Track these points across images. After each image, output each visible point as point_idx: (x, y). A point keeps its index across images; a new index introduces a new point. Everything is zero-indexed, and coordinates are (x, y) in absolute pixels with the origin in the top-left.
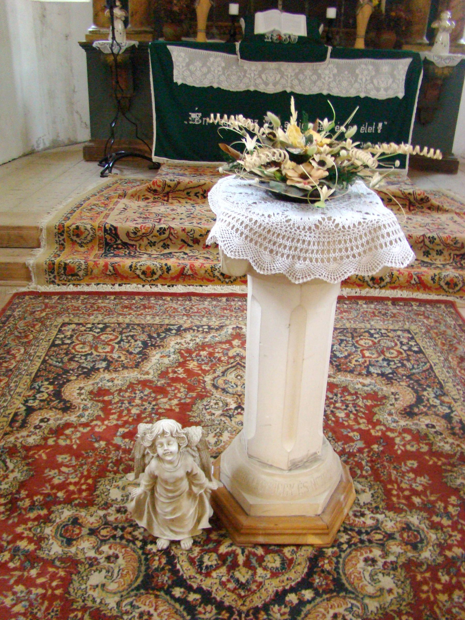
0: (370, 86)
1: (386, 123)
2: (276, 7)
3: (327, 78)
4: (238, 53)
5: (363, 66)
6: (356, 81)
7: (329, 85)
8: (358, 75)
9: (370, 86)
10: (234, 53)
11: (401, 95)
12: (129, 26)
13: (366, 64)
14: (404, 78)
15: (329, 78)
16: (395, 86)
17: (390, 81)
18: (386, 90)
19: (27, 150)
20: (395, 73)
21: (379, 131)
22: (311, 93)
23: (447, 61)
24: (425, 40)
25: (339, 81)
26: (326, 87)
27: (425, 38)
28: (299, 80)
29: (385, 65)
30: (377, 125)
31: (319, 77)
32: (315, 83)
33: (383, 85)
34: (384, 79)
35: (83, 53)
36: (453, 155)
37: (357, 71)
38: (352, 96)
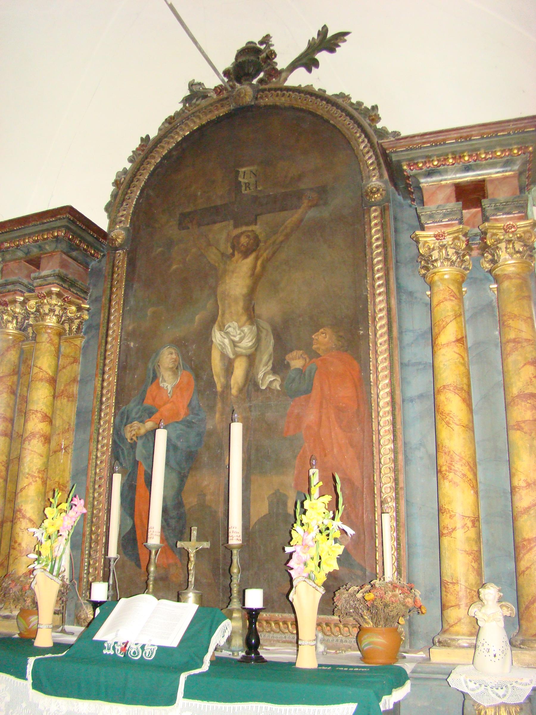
2: (144, 589)
4: (29, 676)
10: (22, 675)
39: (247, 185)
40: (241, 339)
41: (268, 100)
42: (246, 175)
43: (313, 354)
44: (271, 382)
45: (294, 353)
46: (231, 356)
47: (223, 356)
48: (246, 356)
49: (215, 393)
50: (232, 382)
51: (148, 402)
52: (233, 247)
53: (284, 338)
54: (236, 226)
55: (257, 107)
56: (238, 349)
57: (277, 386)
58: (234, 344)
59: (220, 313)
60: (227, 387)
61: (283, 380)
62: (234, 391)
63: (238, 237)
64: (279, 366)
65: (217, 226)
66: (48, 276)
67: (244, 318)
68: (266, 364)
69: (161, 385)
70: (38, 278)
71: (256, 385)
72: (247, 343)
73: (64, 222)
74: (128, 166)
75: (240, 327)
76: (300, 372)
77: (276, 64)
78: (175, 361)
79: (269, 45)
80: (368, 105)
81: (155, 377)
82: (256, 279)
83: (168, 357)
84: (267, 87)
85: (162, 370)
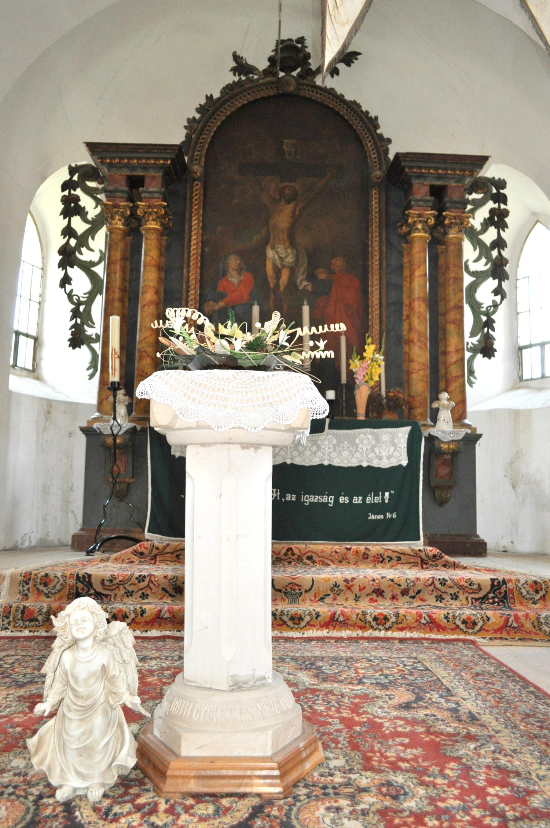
0: (371, 455)
1: (392, 492)
3: (327, 449)
5: (363, 436)
6: (356, 451)
7: (329, 455)
8: (357, 446)
9: (371, 455)
11: (405, 463)
12: (133, 413)
13: (365, 434)
14: (406, 445)
15: (329, 448)
16: (397, 454)
17: (392, 449)
18: (389, 458)
19: (11, 545)
20: (396, 441)
21: (387, 501)
22: (312, 464)
23: (452, 435)
24: (429, 422)
25: (340, 451)
26: (327, 458)
27: (429, 420)
28: (299, 451)
29: (385, 434)
30: (383, 495)
31: (319, 447)
32: (315, 453)
33: (384, 454)
34: (385, 448)
35: (82, 439)
36: (478, 536)
37: (357, 441)
38: (354, 465)
39: (290, 154)
40: (286, 257)
41: (306, 93)
42: (288, 145)
43: (331, 272)
44: (305, 286)
45: (320, 270)
46: (280, 267)
47: (275, 266)
48: (289, 267)
49: (270, 288)
50: (281, 282)
51: (220, 289)
52: (280, 195)
53: (315, 259)
54: (282, 181)
55: (298, 97)
56: (284, 263)
57: (309, 288)
58: (281, 259)
59: (272, 237)
60: (277, 285)
61: (313, 285)
62: (282, 289)
63: (284, 188)
64: (311, 277)
65: (267, 178)
66: (156, 192)
67: (288, 244)
68: (303, 274)
69: (230, 279)
70: (145, 192)
71: (296, 286)
72: (290, 260)
73: (174, 156)
74: (198, 116)
75: (285, 249)
76: (323, 281)
77: (310, 64)
78: (240, 264)
79: (304, 47)
80: (372, 114)
81: (225, 274)
82: (295, 219)
83: (233, 262)
84: (305, 82)
85: (230, 270)
